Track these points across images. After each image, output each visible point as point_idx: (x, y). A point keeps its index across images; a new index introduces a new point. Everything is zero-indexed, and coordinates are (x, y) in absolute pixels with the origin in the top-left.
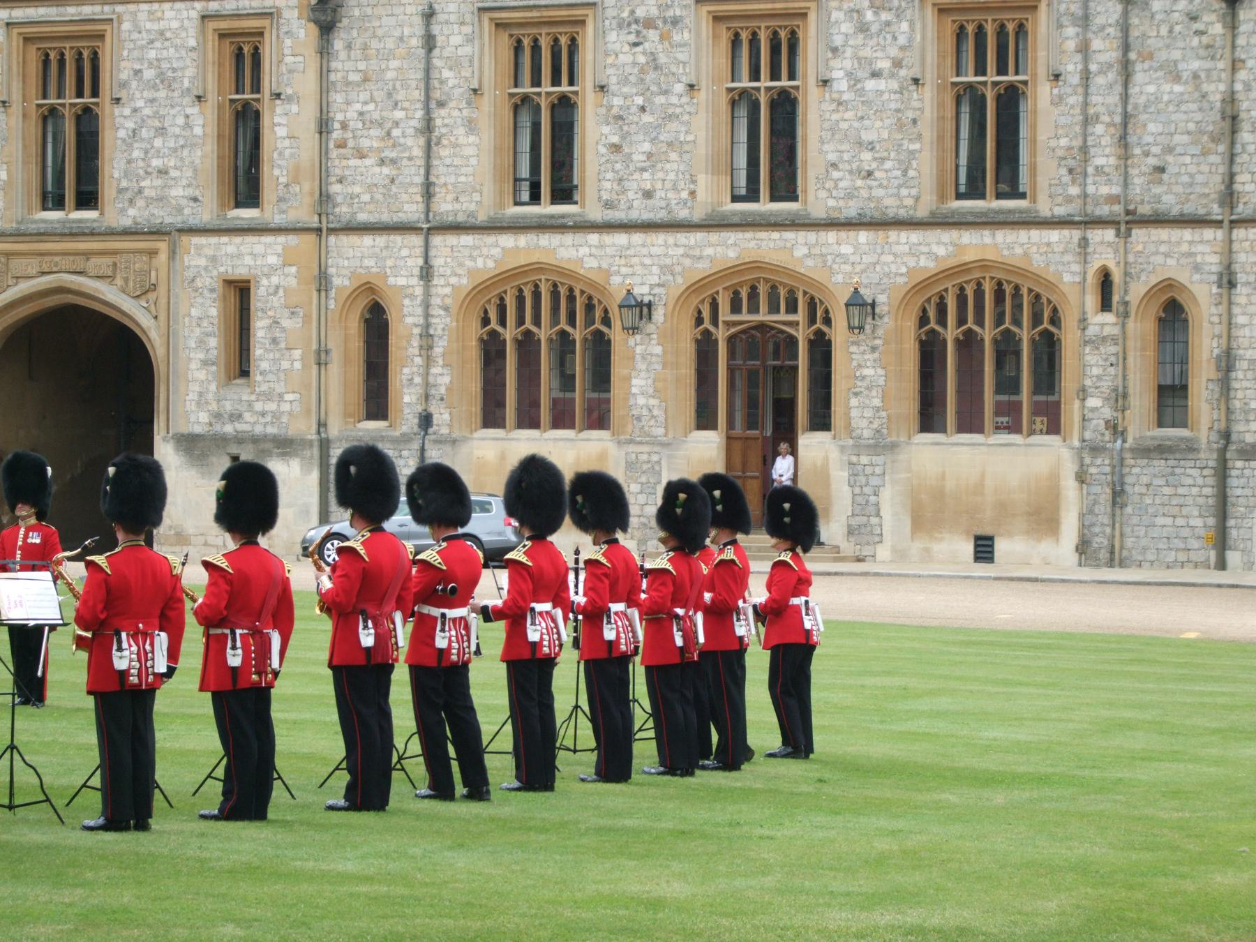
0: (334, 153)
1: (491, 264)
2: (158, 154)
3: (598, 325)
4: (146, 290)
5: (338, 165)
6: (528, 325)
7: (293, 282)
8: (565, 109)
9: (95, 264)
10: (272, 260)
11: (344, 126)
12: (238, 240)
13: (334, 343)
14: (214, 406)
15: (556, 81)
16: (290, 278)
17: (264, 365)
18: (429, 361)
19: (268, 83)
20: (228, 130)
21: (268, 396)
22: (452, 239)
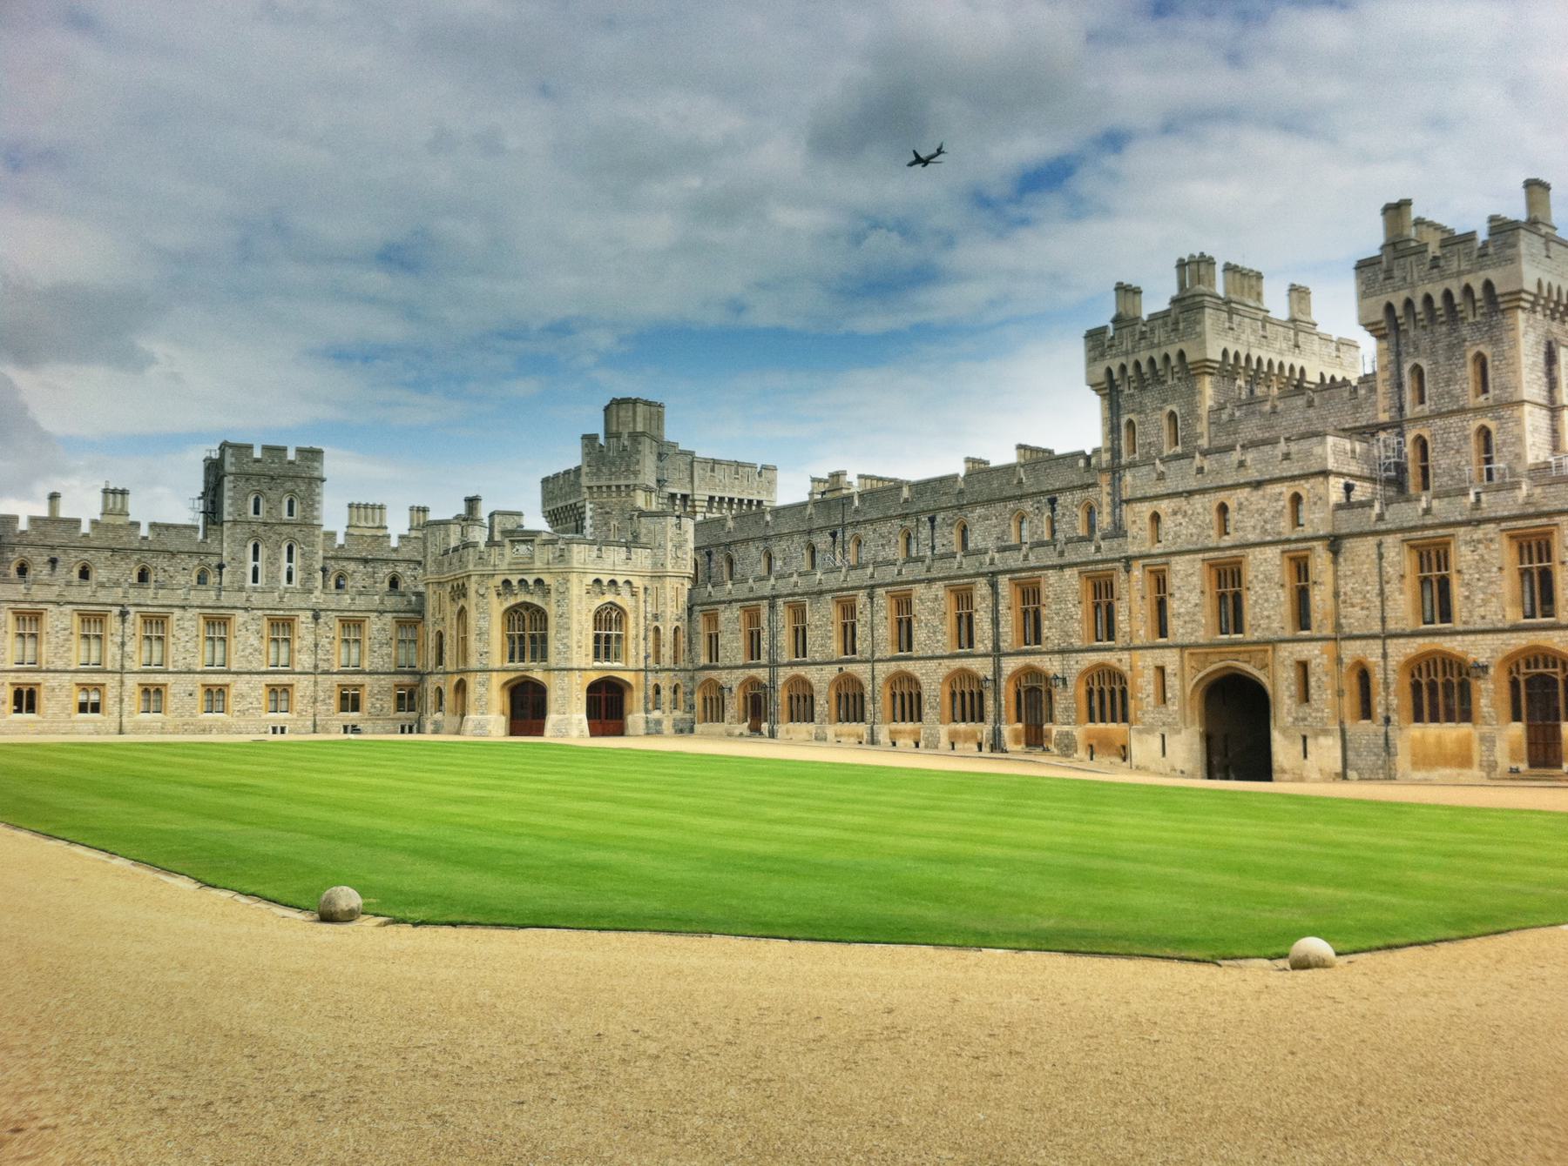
0: (1341, 606)
1: (1413, 650)
2: (1266, 610)
3: (1464, 676)
4: (1264, 667)
5: (1343, 611)
6: (1433, 677)
7: (1325, 662)
8: (1444, 584)
9: (1240, 657)
10: (1317, 652)
11: (1345, 594)
12: (1301, 644)
13: (1346, 688)
14: (1294, 715)
15: (1439, 570)
16: (1325, 659)
17: (1315, 697)
18: (1388, 694)
19: (1312, 577)
20: (1295, 597)
21: (1317, 710)
22: (1395, 641)
